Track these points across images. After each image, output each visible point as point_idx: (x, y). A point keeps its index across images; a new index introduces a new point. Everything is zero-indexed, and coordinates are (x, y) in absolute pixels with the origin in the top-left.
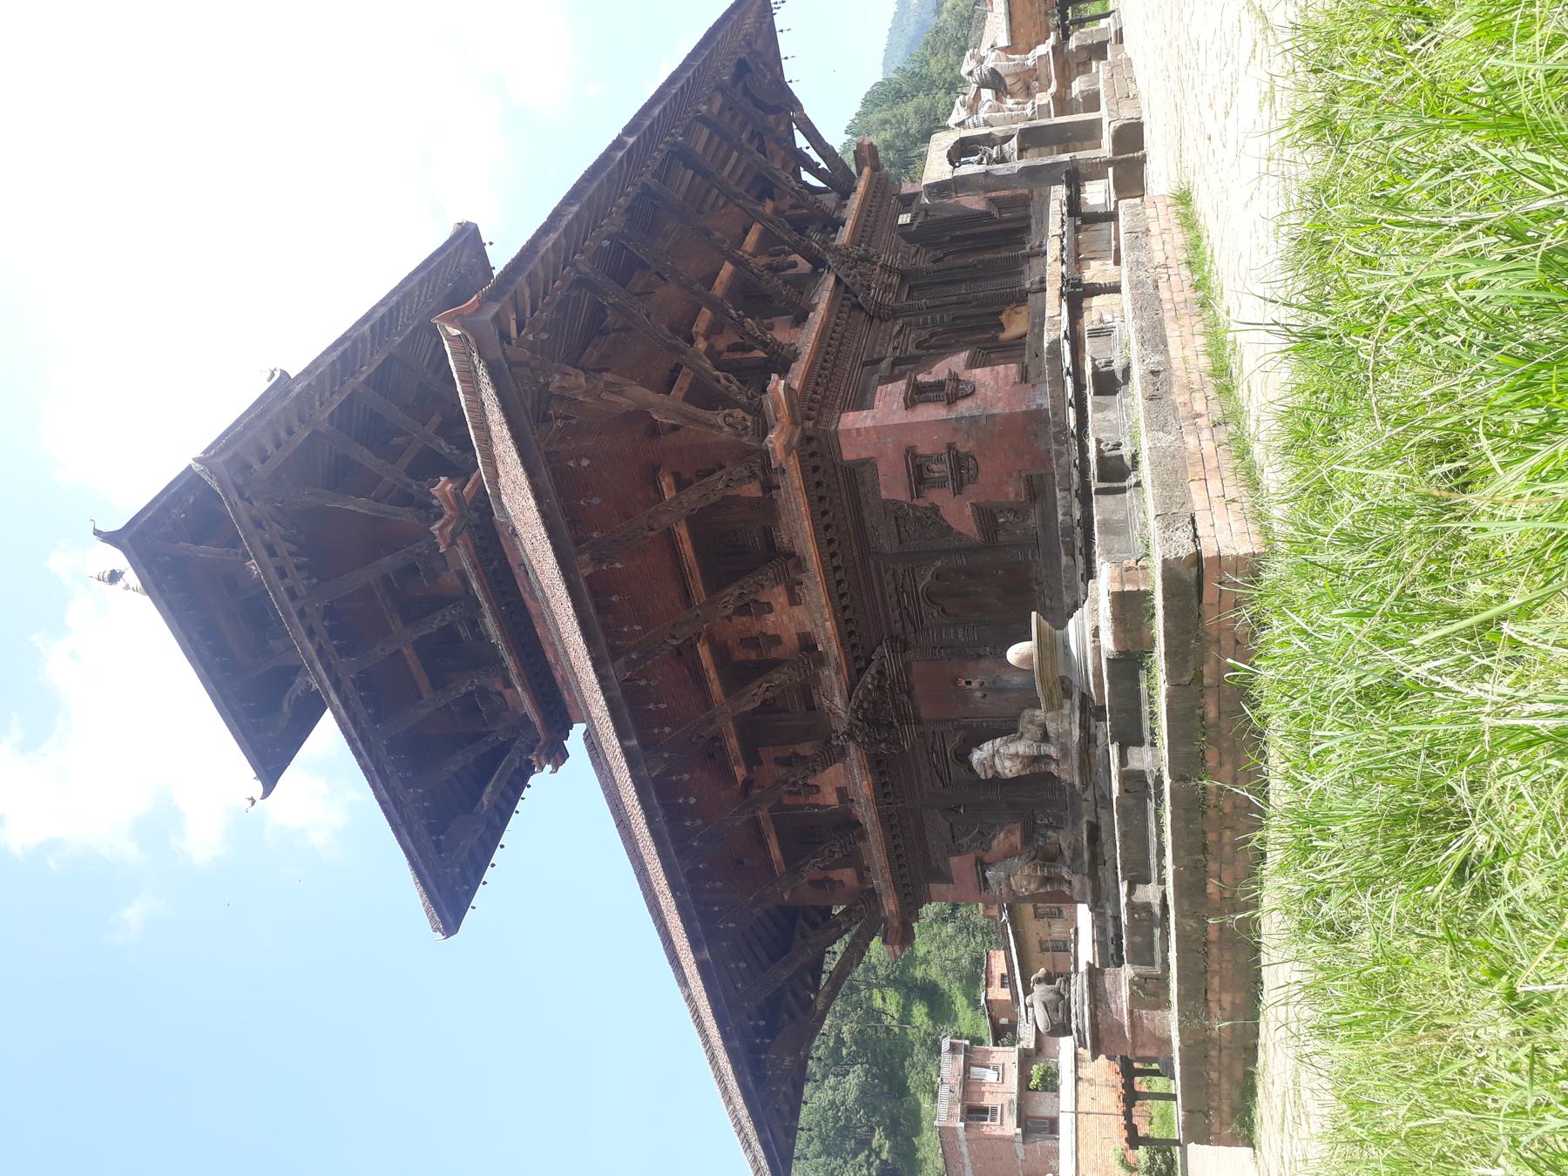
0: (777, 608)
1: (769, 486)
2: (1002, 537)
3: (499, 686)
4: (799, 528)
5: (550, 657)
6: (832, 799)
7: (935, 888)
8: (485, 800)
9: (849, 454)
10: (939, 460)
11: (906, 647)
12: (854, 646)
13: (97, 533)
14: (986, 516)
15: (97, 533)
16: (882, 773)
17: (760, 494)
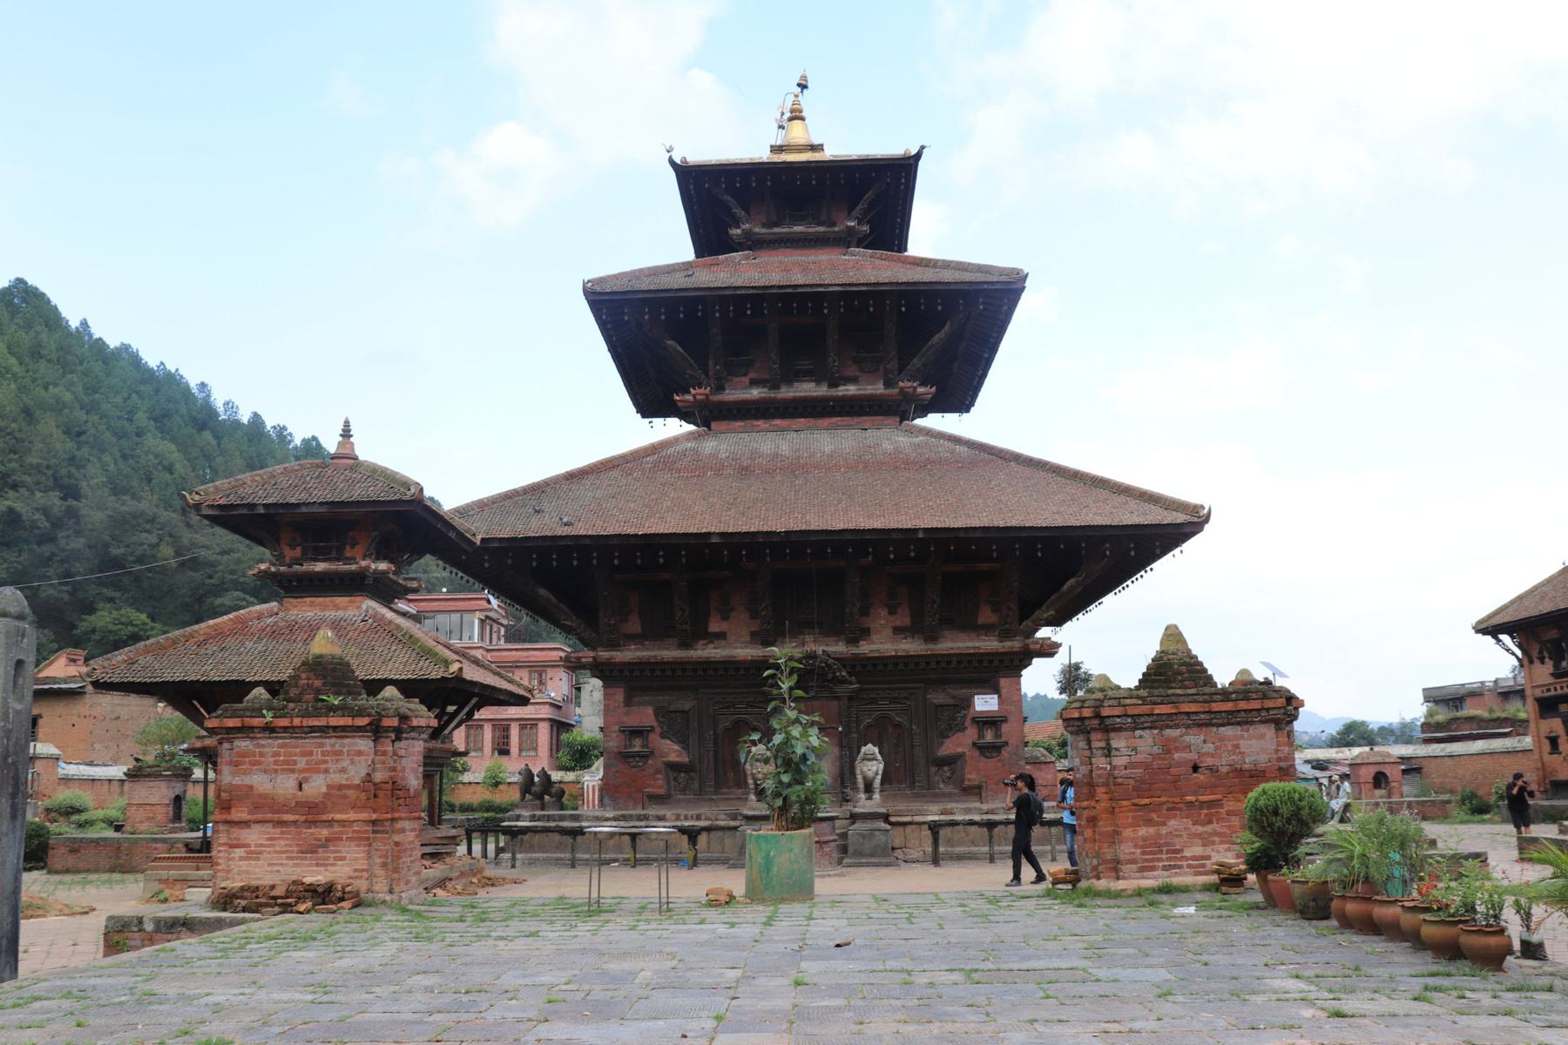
0: (892, 618)
1: (987, 629)
2: (933, 769)
3: (752, 375)
4: (955, 644)
5: (777, 422)
6: (714, 627)
7: (619, 695)
8: (670, 342)
9: (1003, 682)
10: (998, 735)
11: (850, 699)
12: (864, 666)
13: (923, 148)
14: (952, 761)
15: (923, 148)
16: (747, 669)
17: (980, 621)
